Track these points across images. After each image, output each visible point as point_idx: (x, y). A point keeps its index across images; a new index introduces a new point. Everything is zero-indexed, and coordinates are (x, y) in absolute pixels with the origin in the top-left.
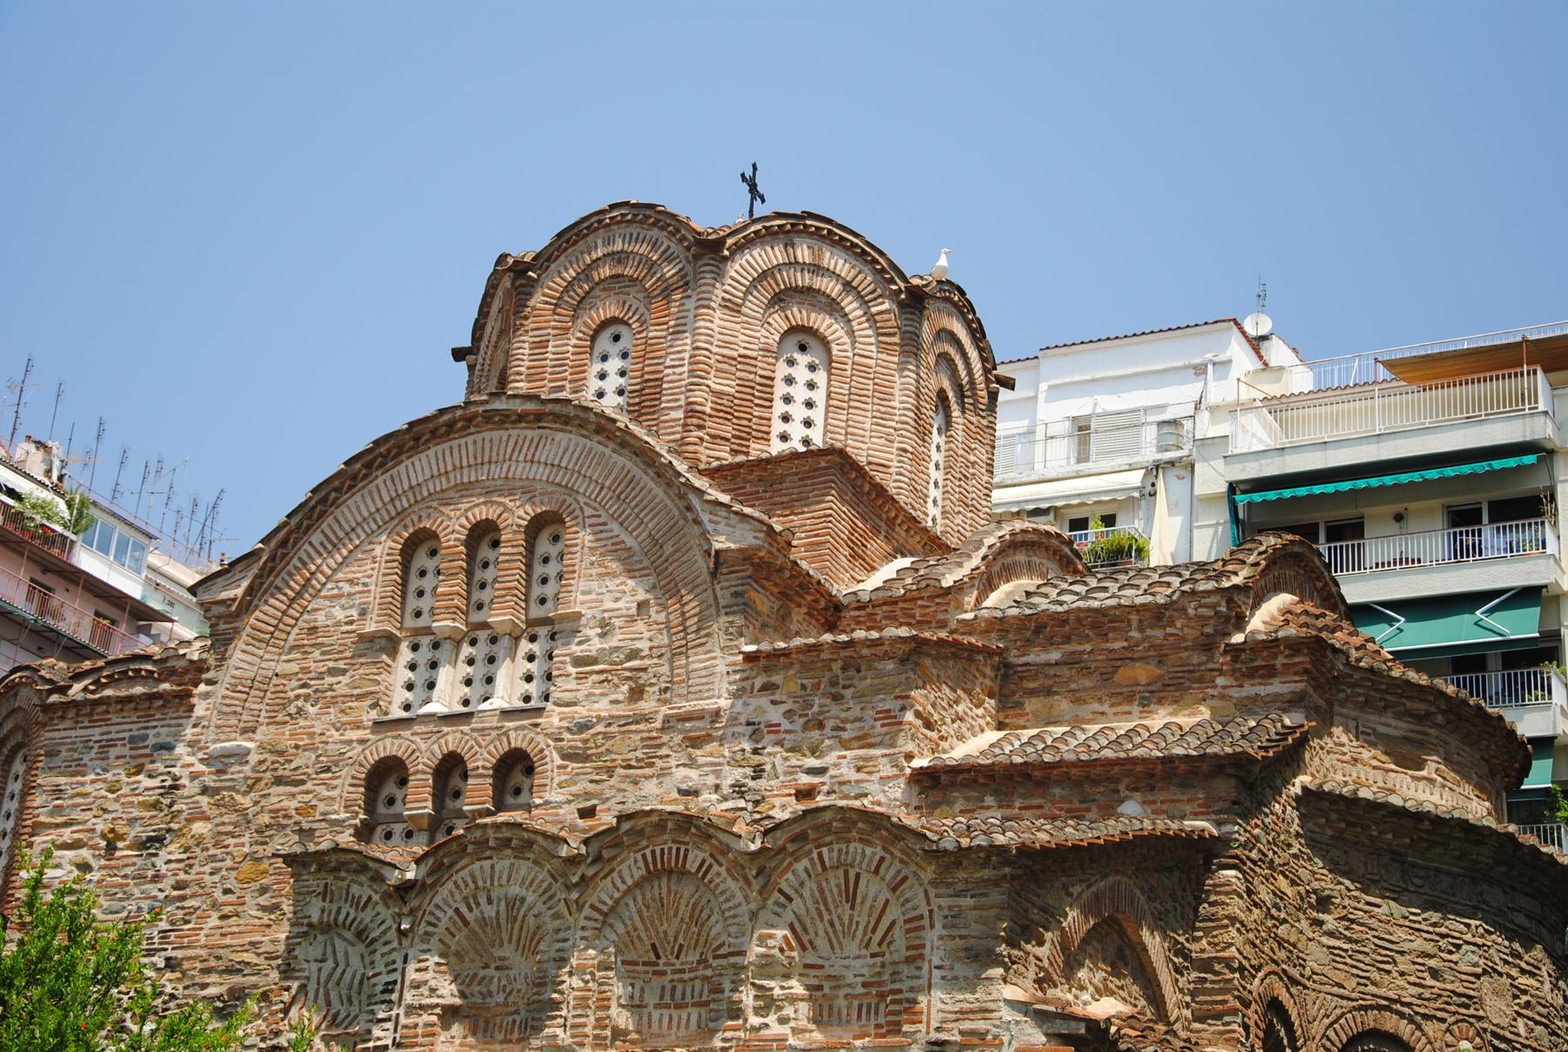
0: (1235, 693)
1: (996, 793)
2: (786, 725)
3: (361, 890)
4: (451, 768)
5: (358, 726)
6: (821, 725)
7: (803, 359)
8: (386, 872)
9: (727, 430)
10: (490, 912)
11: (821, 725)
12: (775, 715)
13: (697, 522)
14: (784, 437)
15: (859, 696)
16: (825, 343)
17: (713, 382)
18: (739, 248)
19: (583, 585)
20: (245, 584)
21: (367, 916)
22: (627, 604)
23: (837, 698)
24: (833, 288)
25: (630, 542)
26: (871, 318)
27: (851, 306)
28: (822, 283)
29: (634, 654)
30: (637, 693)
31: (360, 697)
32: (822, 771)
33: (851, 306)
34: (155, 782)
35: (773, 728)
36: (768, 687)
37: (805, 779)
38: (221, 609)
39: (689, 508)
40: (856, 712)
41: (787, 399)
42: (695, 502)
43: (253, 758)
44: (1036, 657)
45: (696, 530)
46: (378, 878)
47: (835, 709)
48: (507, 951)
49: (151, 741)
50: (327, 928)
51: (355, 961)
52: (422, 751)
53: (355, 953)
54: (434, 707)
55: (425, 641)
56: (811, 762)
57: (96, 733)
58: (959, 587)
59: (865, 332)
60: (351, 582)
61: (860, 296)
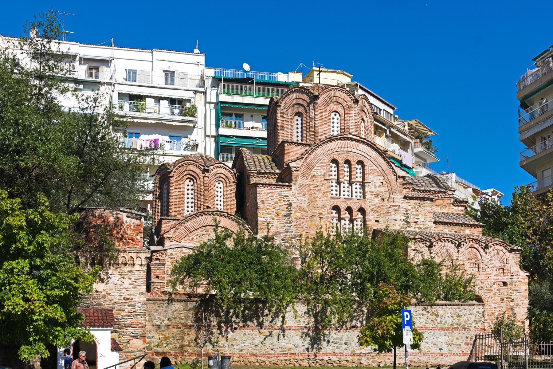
0: (454, 208)
3: (421, 244)
5: (327, 197)
10: (444, 251)
12: (410, 208)
13: (393, 169)
19: (370, 177)
20: (301, 164)
21: (423, 249)
22: (379, 182)
29: (381, 192)
34: (286, 203)
36: (408, 203)
37: (416, 220)
38: (295, 169)
39: (391, 166)
43: (307, 201)
47: (420, 208)
49: (283, 194)
57: (270, 191)
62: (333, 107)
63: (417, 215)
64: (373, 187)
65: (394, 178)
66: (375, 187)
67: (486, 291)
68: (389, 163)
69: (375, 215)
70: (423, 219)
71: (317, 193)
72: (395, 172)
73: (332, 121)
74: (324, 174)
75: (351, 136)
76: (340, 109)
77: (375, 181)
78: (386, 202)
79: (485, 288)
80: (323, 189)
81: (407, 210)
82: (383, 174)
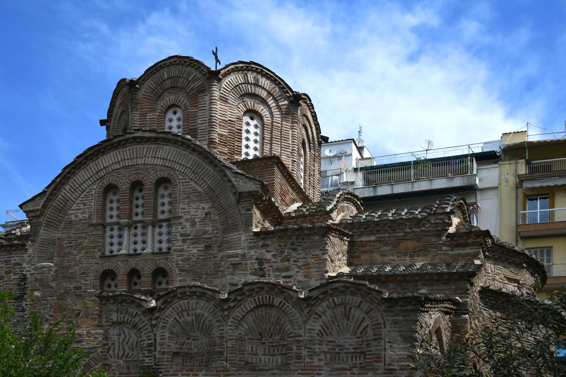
4: (134, 273)
12: (269, 256)
22: (201, 213)
24: (264, 94)
30: (208, 247)
36: (264, 246)
52: (122, 269)
54: (123, 252)
62: (169, 98)
63: (287, 269)
65: (233, 199)
66: (193, 224)
80: (86, 243)
81: (261, 261)
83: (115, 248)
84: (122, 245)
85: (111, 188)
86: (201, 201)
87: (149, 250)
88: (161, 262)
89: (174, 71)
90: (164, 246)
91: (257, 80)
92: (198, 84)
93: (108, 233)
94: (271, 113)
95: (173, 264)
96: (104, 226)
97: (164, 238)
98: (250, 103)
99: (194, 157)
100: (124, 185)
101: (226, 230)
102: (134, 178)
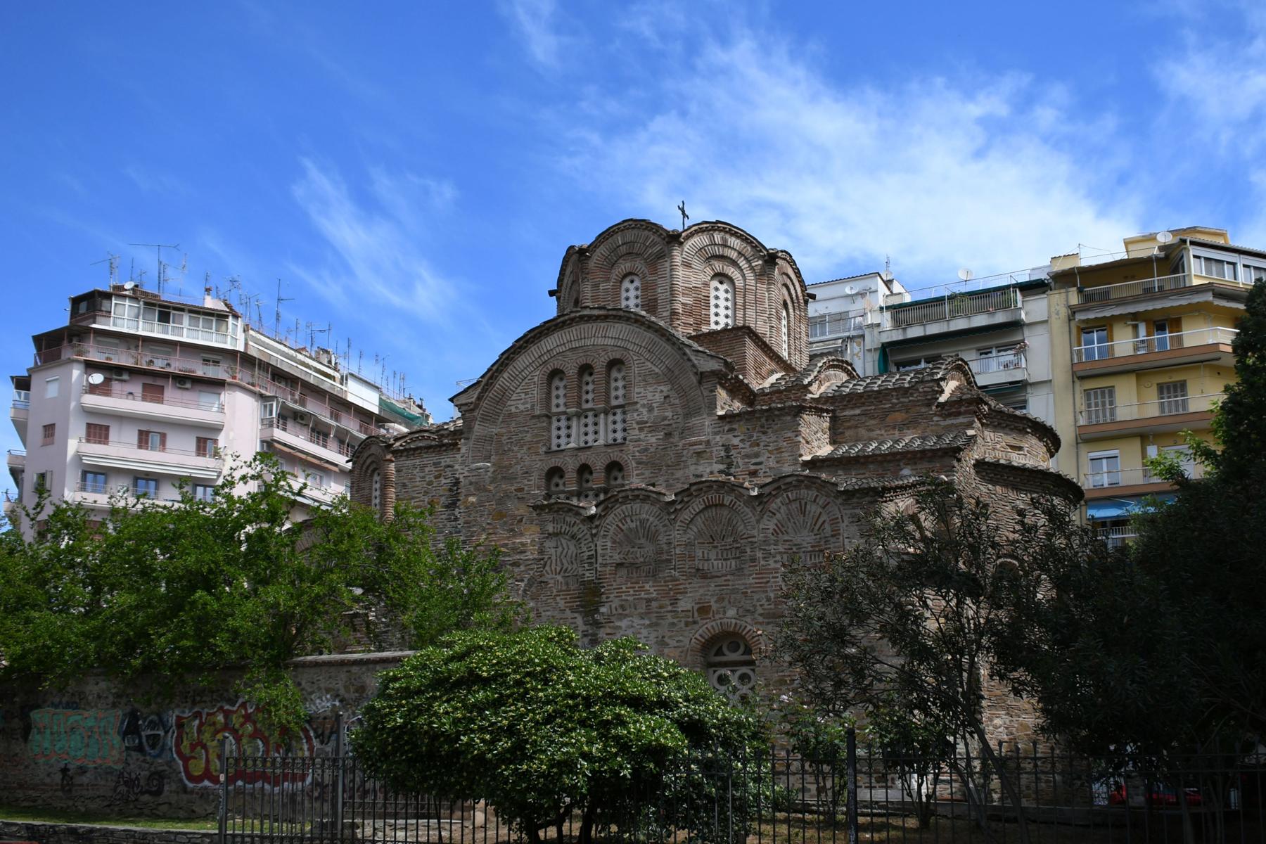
1: (843, 469)
2: (741, 445)
6: (758, 445)
7: (723, 287)
8: (582, 511)
9: (691, 321)
11: (758, 445)
12: (736, 441)
13: (689, 360)
14: (717, 323)
15: (775, 432)
16: (731, 280)
17: (682, 299)
18: (688, 238)
19: (637, 390)
21: (575, 529)
22: (659, 397)
23: (764, 433)
24: (734, 255)
25: (657, 370)
26: (752, 268)
27: (742, 263)
28: (728, 252)
29: (665, 418)
30: (668, 435)
31: (538, 442)
32: (760, 463)
33: (742, 263)
35: (735, 447)
36: (731, 430)
37: (753, 467)
39: (685, 354)
40: (774, 438)
41: (717, 306)
42: (687, 351)
44: (848, 413)
45: (689, 364)
46: (578, 514)
47: (764, 438)
48: (643, 541)
50: (556, 535)
51: (572, 548)
52: (570, 465)
53: (572, 544)
54: (572, 445)
55: (563, 417)
56: (754, 461)
58: (810, 384)
59: (750, 276)
60: (526, 394)
61: (746, 259)
63: (757, 455)
64: (644, 411)
65: (694, 379)
66: (651, 409)
67: (761, 619)
68: (680, 349)
69: (647, 473)
70: (772, 463)
71: (516, 449)
72: (694, 366)
73: (624, 295)
74: (533, 406)
75: (586, 312)
76: (639, 265)
77: (650, 396)
78: (675, 439)
79: (760, 611)
80: (528, 437)
81: (727, 448)
82: (670, 377)
83: (563, 441)
84: (569, 437)
85: (556, 374)
86: (658, 383)
87: (601, 442)
88: (615, 455)
89: (629, 236)
90: (619, 435)
91: (725, 240)
92: (657, 249)
93: (555, 424)
94: (744, 276)
95: (629, 457)
96: (549, 417)
97: (619, 426)
98: (718, 266)
99: (649, 335)
100: (571, 370)
101: (688, 415)
102: (582, 361)
